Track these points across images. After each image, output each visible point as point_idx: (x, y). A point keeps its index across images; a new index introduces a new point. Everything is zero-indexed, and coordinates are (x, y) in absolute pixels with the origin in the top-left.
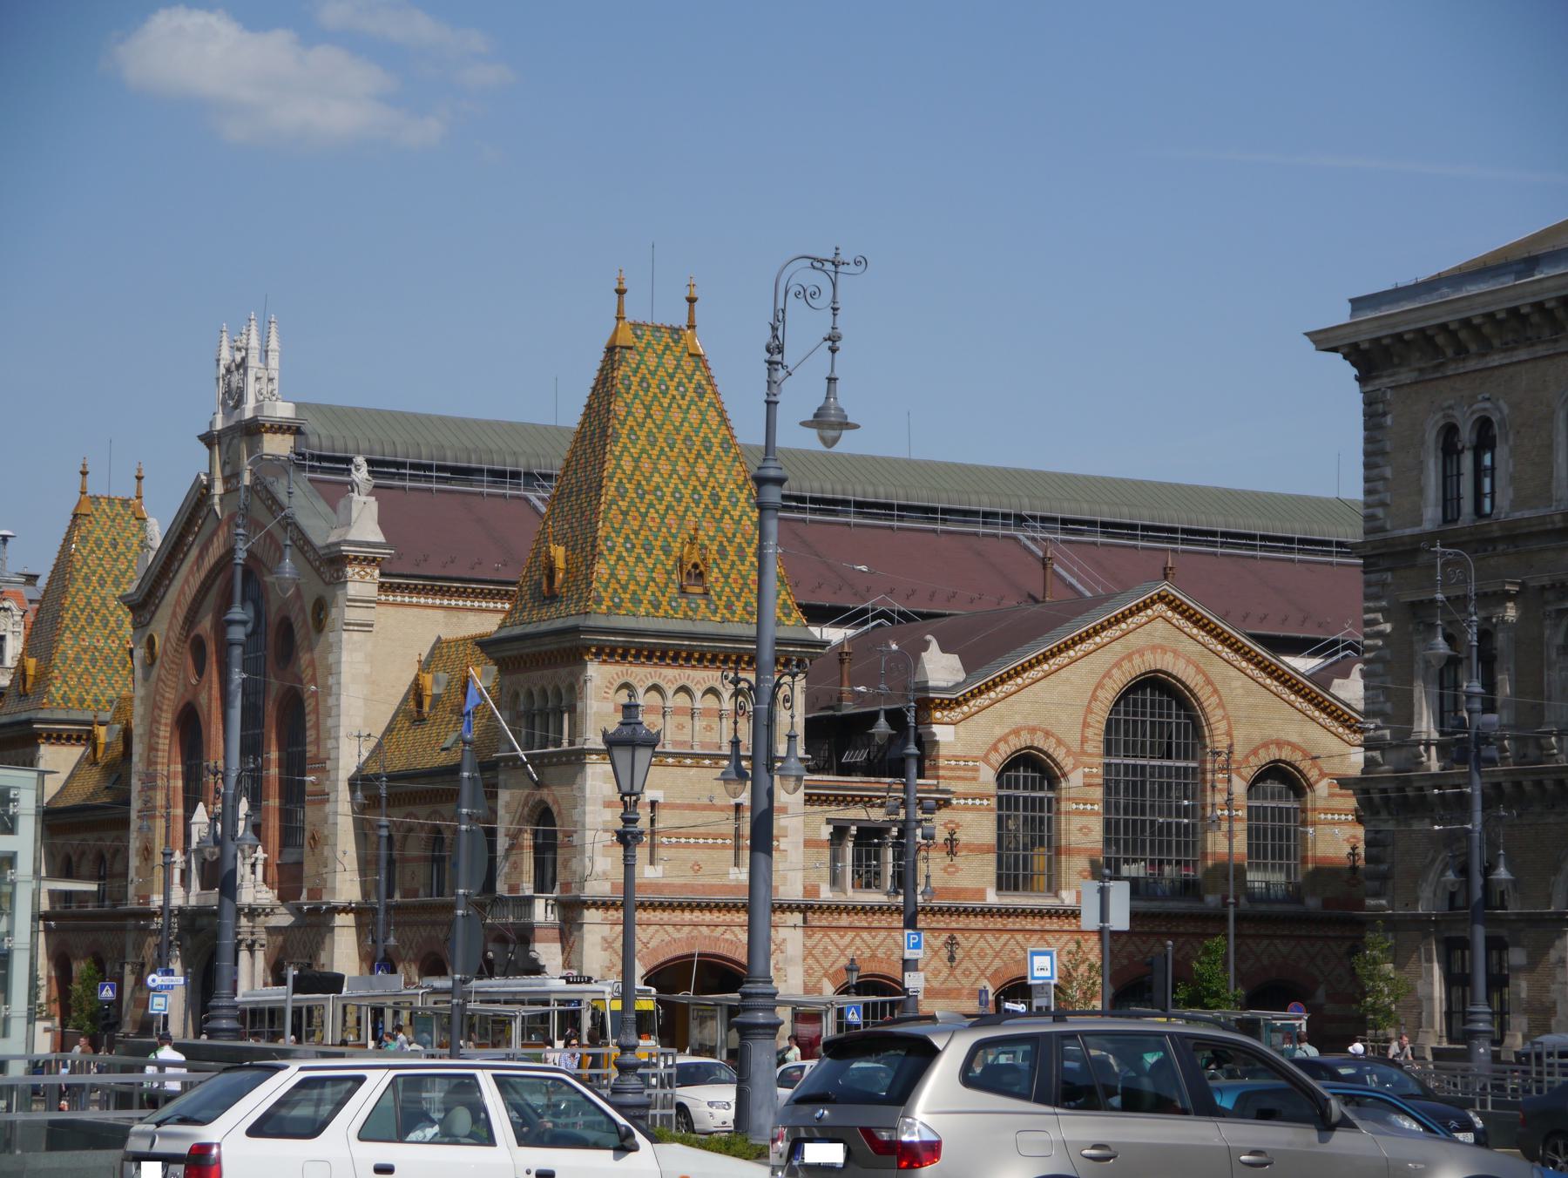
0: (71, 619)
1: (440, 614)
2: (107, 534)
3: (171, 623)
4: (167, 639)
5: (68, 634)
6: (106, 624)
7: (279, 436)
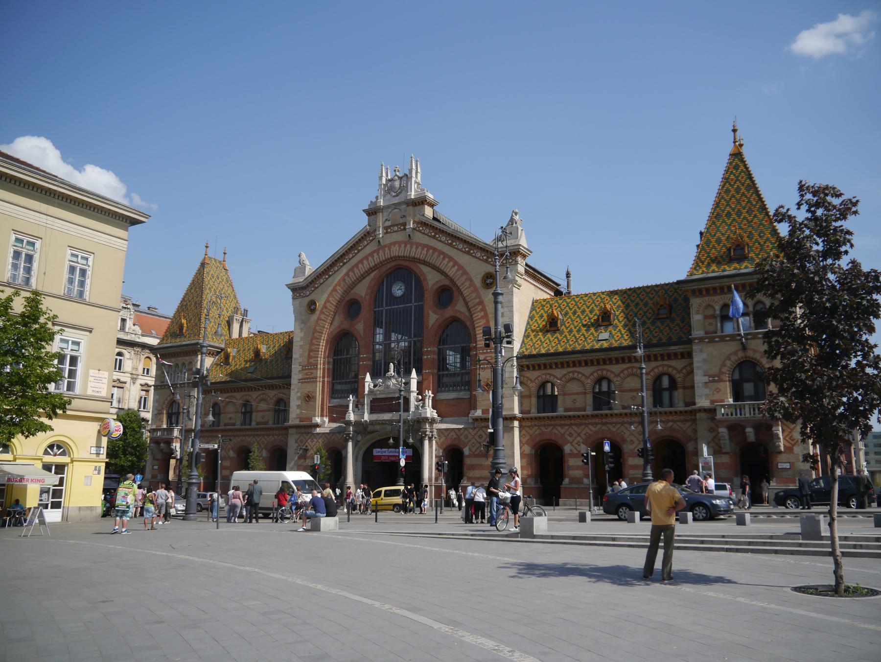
1: (533, 287)
3: (331, 295)
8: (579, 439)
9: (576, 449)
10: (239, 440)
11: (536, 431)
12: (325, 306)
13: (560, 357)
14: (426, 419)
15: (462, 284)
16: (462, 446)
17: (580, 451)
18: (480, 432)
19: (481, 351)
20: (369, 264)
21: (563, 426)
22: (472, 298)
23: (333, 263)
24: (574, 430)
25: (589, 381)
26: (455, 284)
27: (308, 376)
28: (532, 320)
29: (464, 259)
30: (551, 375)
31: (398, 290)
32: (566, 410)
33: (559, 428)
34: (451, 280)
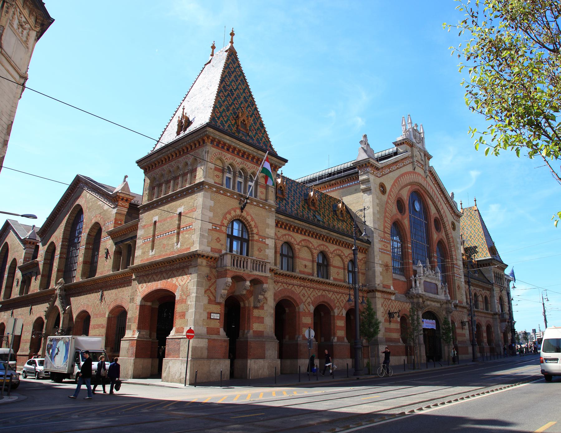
10: (319, 294)
16: (455, 322)
26: (442, 219)
27: (385, 248)
29: (445, 207)
34: (441, 216)
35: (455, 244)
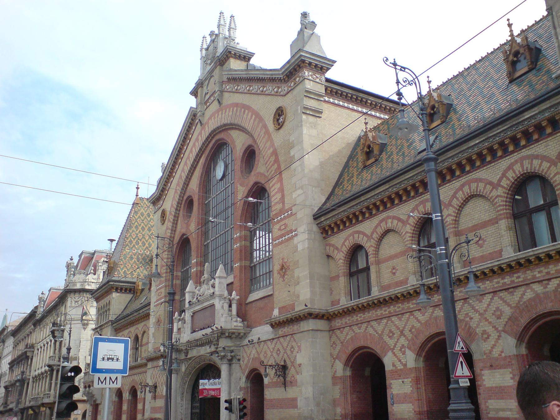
0: (129, 242)
2: (146, 212)
3: (174, 197)
4: (172, 206)
5: (127, 247)
6: (144, 244)
7: (238, 62)
8: (403, 340)
9: (400, 361)
11: (347, 334)
12: (170, 213)
13: (362, 198)
14: (222, 333)
15: (259, 135)
17: (405, 365)
18: (279, 346)
19: (276, 220)
20: (196, 150)
21: (378, 319)
22: (266, 150)
23: (174, 162)
24: (395, 325)
25: (408, 228)
28: (352, 161)
30: (359, 232)
31: (219, 172)
32: (383, 288)
33: (374, 323)
35: (281, 158)
